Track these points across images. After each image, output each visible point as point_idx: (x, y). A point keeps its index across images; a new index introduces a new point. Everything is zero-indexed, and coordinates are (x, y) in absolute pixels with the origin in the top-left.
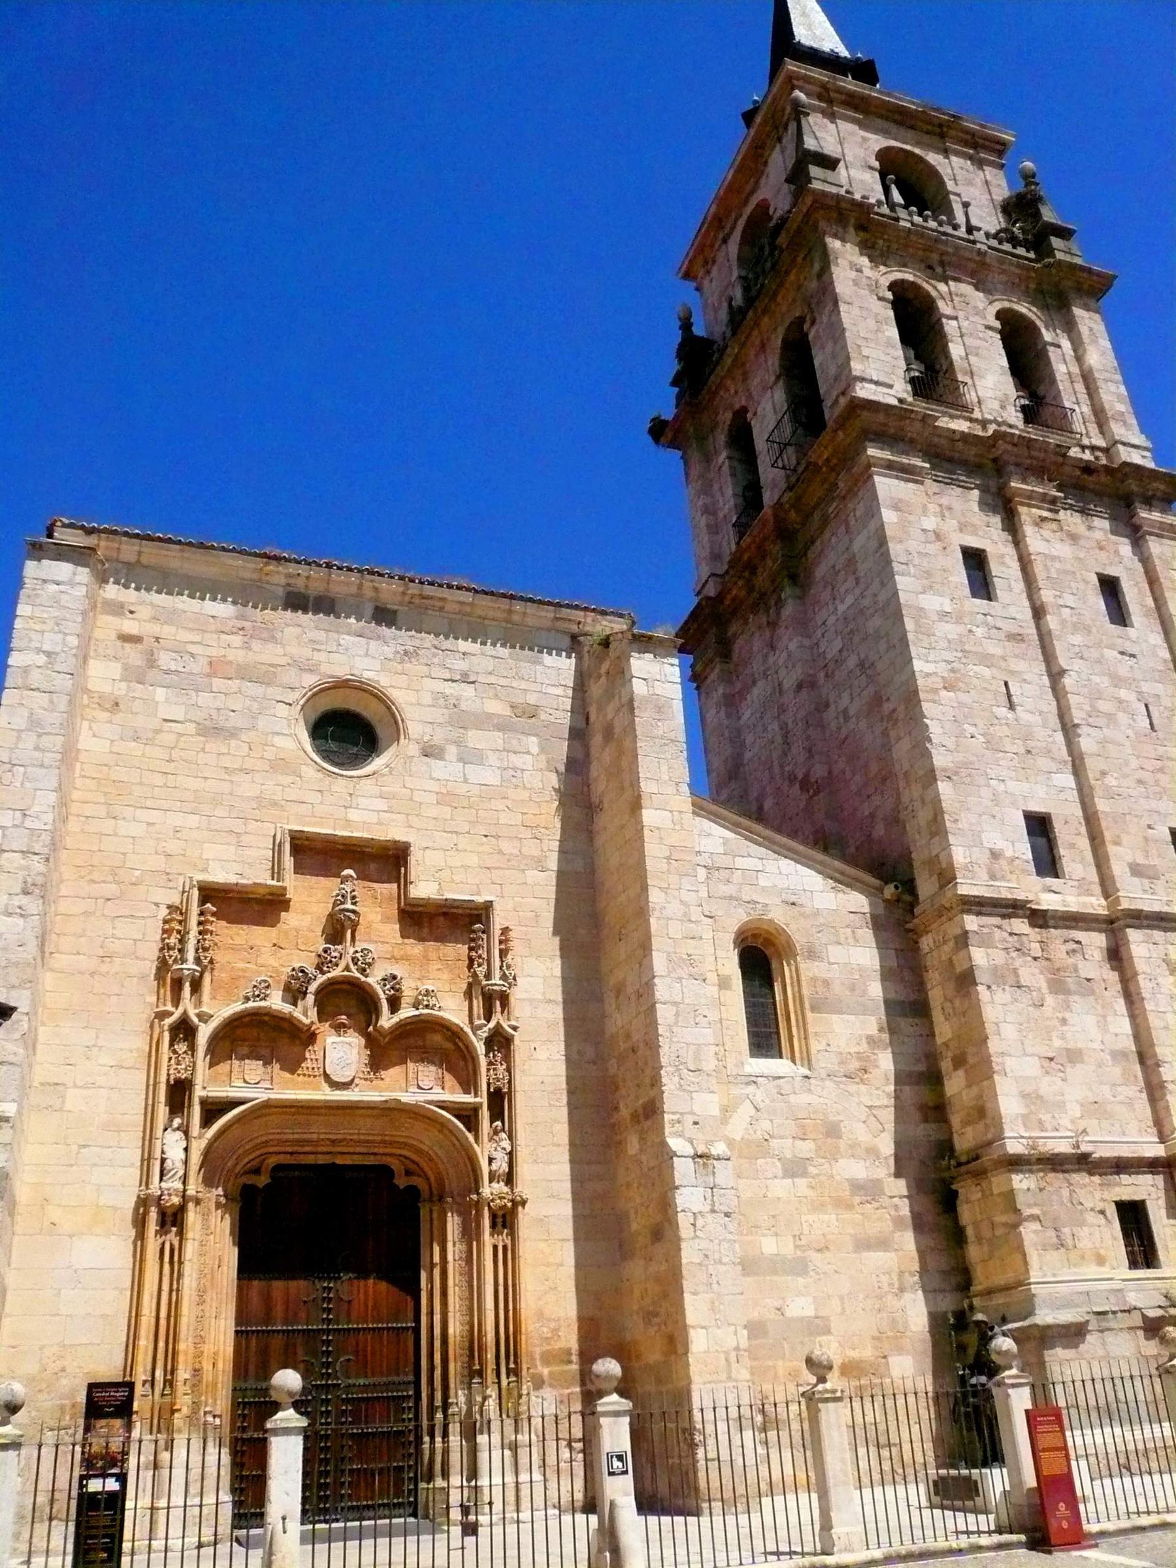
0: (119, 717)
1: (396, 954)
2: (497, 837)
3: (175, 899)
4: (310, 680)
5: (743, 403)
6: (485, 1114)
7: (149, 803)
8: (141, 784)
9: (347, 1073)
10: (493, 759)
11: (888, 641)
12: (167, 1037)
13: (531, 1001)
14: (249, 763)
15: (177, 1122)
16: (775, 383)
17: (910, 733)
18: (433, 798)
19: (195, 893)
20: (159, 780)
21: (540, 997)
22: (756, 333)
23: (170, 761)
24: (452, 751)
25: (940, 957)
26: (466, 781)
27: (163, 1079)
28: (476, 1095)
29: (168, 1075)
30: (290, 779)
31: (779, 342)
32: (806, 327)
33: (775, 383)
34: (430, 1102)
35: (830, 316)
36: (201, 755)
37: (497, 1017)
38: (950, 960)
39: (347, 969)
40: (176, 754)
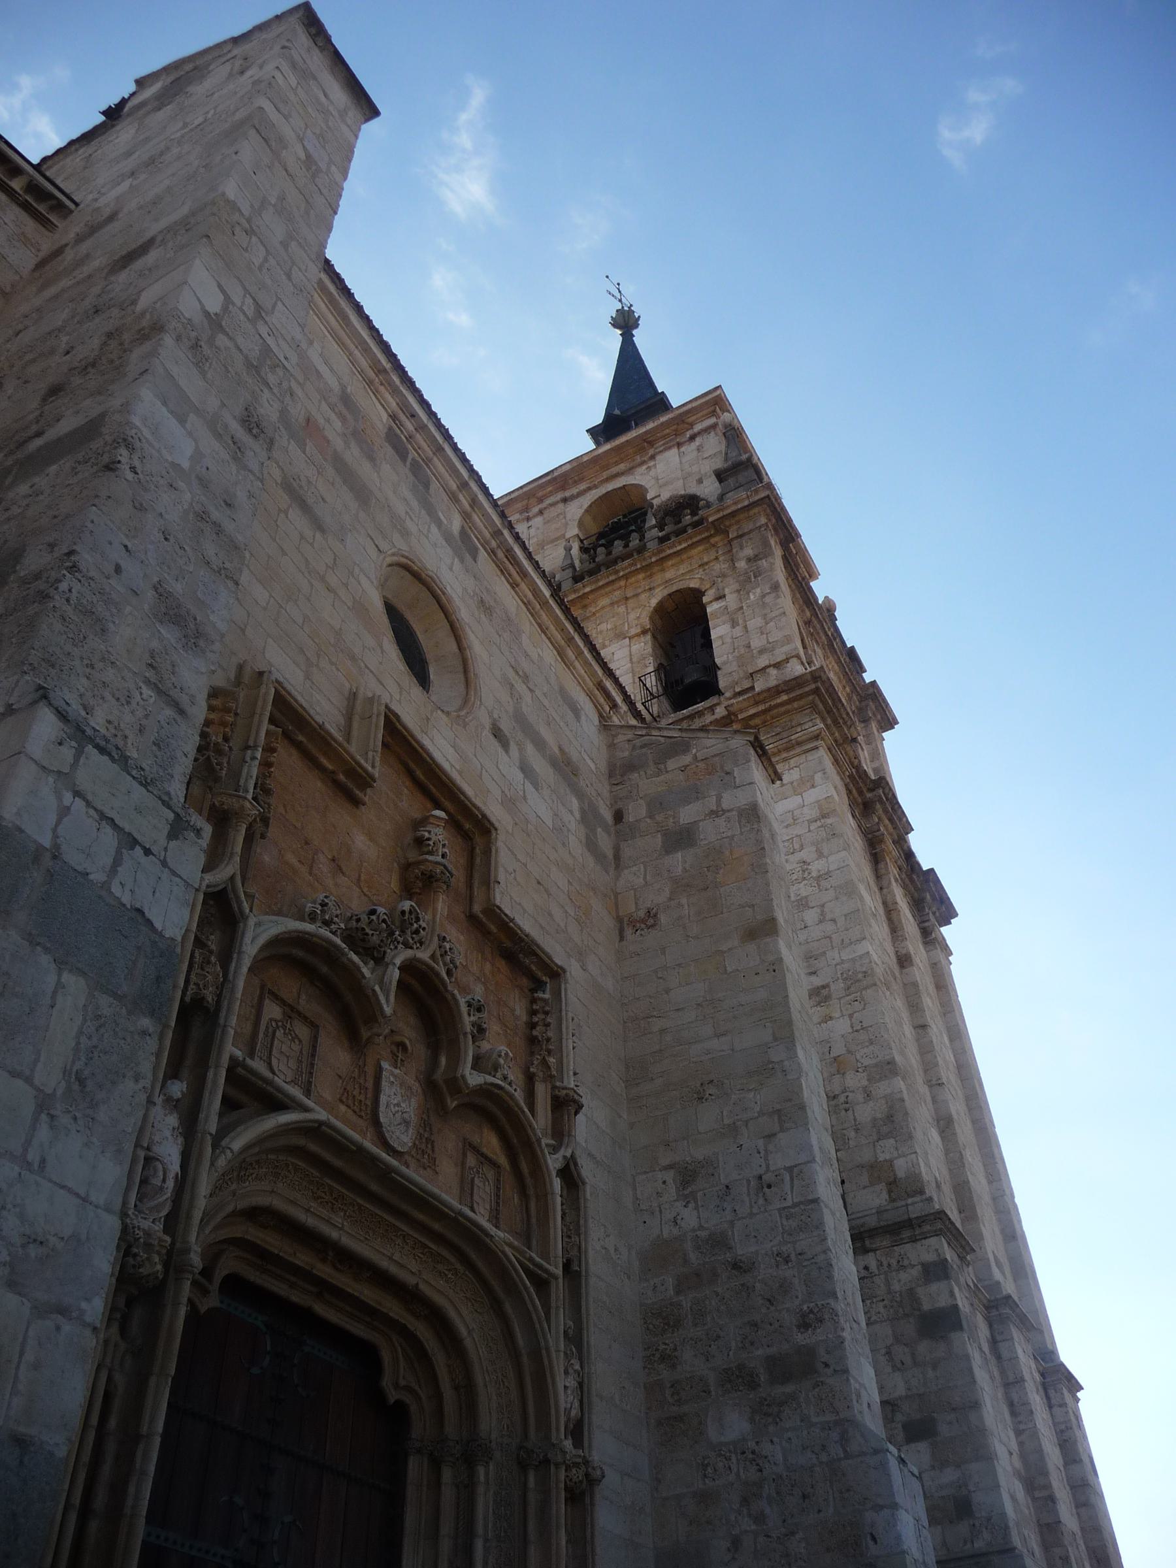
4: (402, 545)
11: (823, 914)
15: (177, 1089)
16: (638, 635)
17: (851, 1016)
22: (622, 583)
25: (888, 1283)
31: (654, 602)
32: (705, 599)
33: (638, 635)
35: (764, 596)
36: (282, 515)
38: (911, 1292)
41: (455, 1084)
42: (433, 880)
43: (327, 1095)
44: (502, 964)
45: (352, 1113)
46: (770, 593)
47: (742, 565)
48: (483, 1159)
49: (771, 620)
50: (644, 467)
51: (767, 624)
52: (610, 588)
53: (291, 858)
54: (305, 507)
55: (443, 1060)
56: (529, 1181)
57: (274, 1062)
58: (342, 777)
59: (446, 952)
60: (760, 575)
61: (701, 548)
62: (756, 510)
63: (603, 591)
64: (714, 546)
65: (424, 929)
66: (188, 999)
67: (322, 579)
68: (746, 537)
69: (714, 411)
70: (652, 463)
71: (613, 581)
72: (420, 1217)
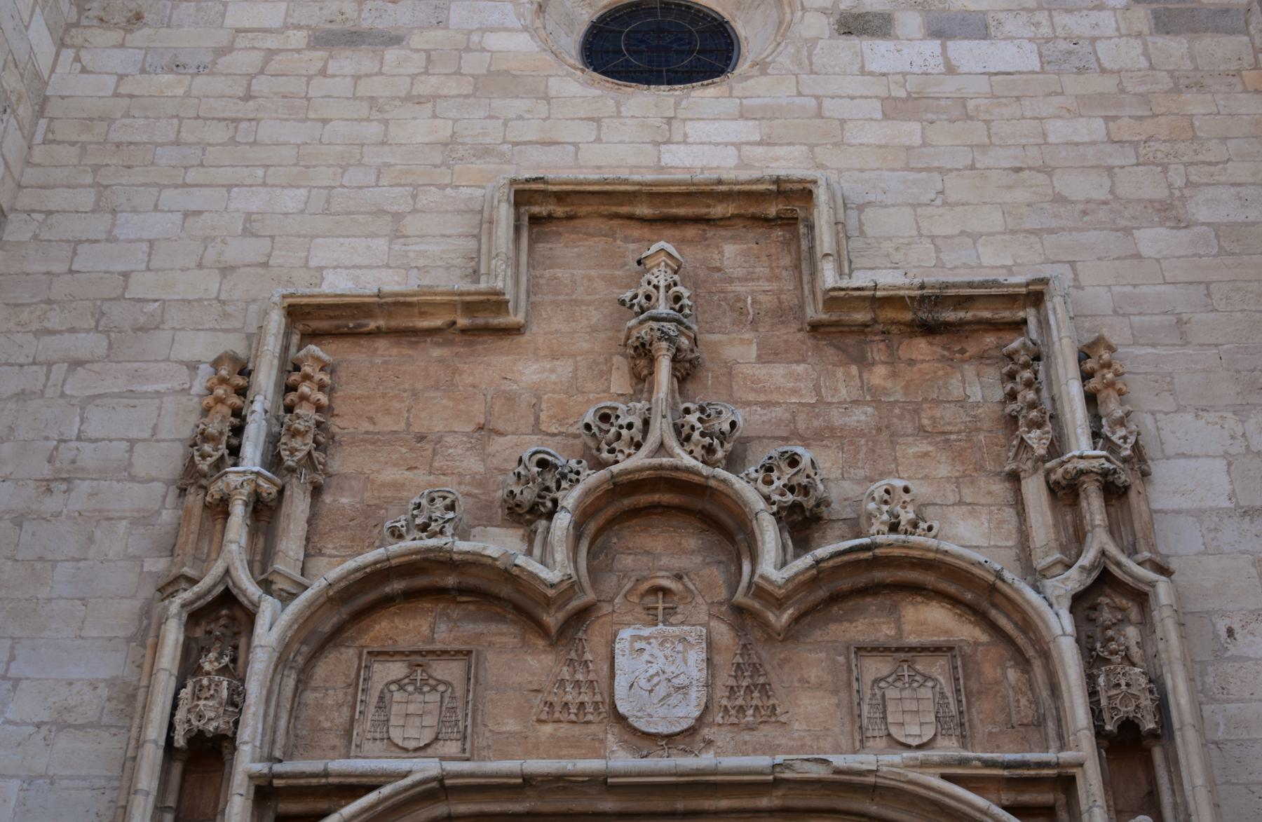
0: (140, 36)
1: (801, 426)
2: (1047, 170)
3: (236, 345)
6: (1091, 785)
7: (193, 176)
8: (177, 143)
9: (680, 711)
10: (1012, 25)
12: (173, 634)
13: (1198, 514)
14: (425, 86)
18: (875, 109)
19: (276, 321)
20: (218, 134)
21: (1227, 504)
23: (248, 97)
24: (910, 22)
26: (951, 70)
27: (155, 732)
28: (1062, 748)
29: (171, 727)
30: (520, 105)
34: (925, 764)
37: (1099, 540)
39: (661, 447)
40: (260, 86)
41: (760, 591)
42: (648, 347)
43: (511, 726)
44: (921, 348)
45: (569, 726)
48: (902, 655)
53: (390, 474)
54: (354, 38)
55: (746, 568)
56: (1021, 640)
57: (396, 735)
58: (462, 322)
59: (693, 428)
65: (630, 426)
66: (180, 741)
67: (408, 98)
72: (724, 804)
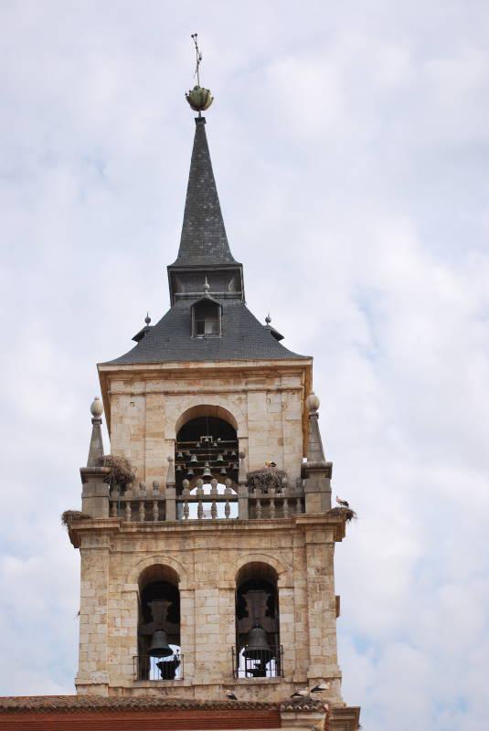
5: (175, 566)
16: (225, 589)
22: (219, 533)
31: (241, 563)
32: (280, 584)
35: (324, 611)
46: (328, 610)
47: (312, 572)
49: (327, 635)
50: (237, 396)
51: (323, 637)
52: (208, 534)
60: (323, 590)
61: (282, 533)
62: (329, 527)
63: (202, 534)
64: (291, 535)
68: (318, 547)
69: (301, 373)
70: (243, 396)
71: (212, 531)
